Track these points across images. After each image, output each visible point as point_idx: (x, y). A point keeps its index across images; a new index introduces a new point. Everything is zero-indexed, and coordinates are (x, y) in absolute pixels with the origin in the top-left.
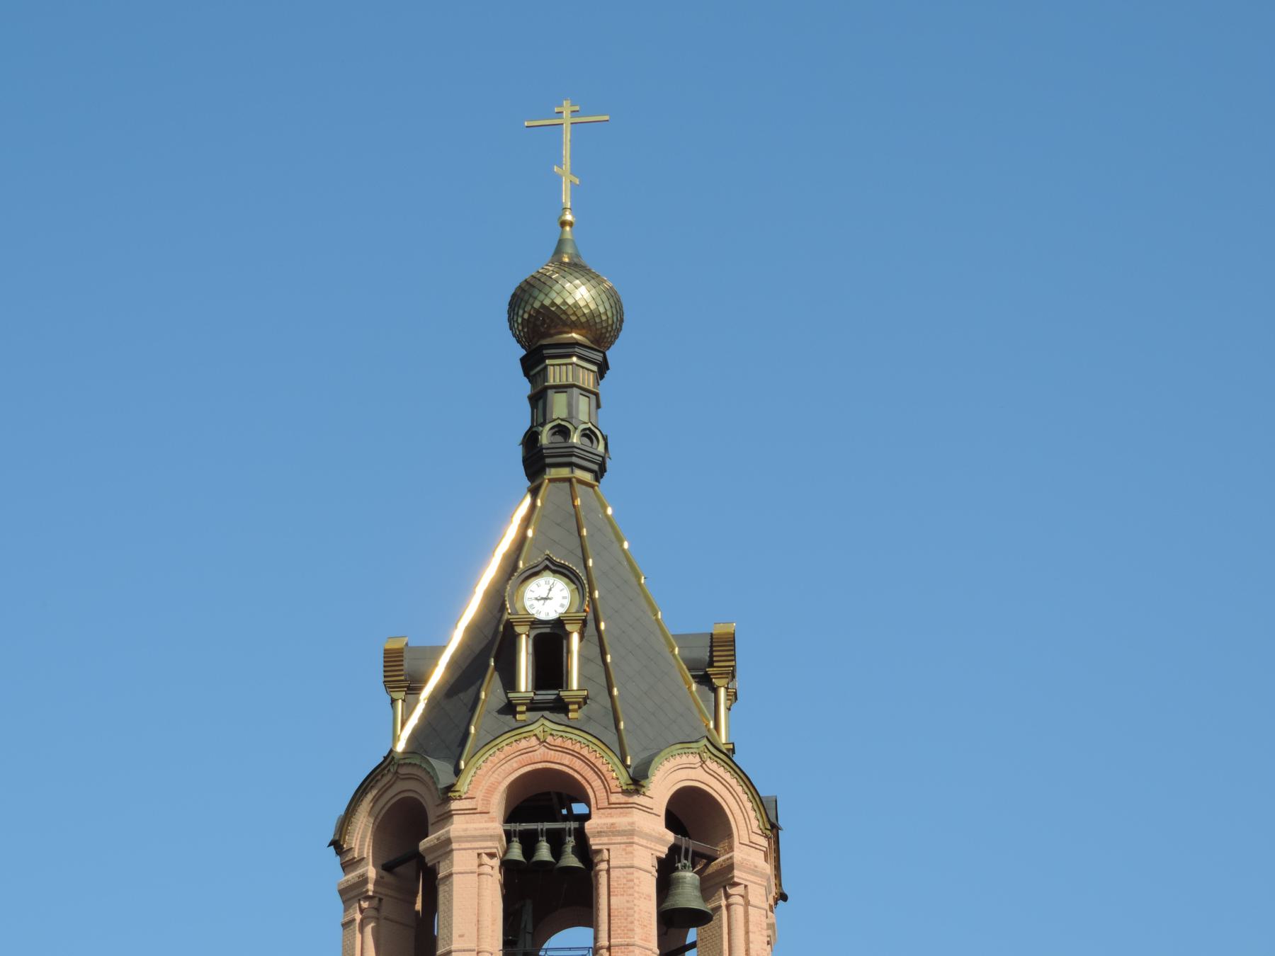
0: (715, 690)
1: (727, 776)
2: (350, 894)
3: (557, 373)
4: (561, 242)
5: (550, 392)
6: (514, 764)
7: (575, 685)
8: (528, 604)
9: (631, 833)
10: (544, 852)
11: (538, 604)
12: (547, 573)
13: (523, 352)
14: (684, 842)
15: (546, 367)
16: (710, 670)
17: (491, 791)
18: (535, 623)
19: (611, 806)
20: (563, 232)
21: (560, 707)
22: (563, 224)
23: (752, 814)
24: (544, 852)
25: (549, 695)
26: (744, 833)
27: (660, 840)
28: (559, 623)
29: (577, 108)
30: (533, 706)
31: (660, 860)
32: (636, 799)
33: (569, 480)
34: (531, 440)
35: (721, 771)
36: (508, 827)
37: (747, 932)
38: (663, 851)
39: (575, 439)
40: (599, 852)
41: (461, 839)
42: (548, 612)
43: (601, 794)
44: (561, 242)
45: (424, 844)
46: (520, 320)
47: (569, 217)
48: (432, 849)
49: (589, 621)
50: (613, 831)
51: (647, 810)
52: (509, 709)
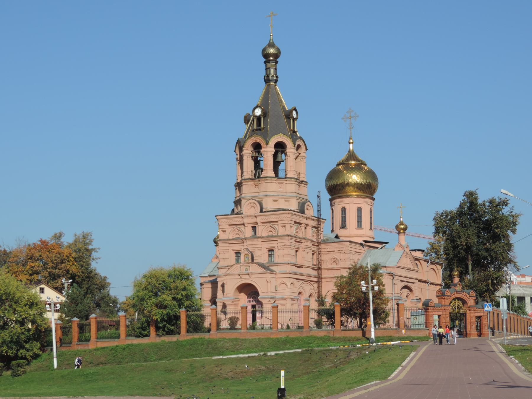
0: (291, 120)
2: (237, 159)
3: (268, 66)
4: (270, 40)
8: (255, 113)
9: (267, 151)
11: (257, 113)
14: (279, 149)
17: (248, 146)
18: (256, 116)
21: (260, 130)
22: (271, 36)
27: (273, 151)
28: (260, 116)
30: (257, 130)
32: (268, 146)
33: (269, 85)
38: (273, 153)
41: (244, 154)
44: (270, 40)
47: (271, 35)
49: (265, 114)
50: (264, 151)
51: (270, 147)
52: (253, 131)
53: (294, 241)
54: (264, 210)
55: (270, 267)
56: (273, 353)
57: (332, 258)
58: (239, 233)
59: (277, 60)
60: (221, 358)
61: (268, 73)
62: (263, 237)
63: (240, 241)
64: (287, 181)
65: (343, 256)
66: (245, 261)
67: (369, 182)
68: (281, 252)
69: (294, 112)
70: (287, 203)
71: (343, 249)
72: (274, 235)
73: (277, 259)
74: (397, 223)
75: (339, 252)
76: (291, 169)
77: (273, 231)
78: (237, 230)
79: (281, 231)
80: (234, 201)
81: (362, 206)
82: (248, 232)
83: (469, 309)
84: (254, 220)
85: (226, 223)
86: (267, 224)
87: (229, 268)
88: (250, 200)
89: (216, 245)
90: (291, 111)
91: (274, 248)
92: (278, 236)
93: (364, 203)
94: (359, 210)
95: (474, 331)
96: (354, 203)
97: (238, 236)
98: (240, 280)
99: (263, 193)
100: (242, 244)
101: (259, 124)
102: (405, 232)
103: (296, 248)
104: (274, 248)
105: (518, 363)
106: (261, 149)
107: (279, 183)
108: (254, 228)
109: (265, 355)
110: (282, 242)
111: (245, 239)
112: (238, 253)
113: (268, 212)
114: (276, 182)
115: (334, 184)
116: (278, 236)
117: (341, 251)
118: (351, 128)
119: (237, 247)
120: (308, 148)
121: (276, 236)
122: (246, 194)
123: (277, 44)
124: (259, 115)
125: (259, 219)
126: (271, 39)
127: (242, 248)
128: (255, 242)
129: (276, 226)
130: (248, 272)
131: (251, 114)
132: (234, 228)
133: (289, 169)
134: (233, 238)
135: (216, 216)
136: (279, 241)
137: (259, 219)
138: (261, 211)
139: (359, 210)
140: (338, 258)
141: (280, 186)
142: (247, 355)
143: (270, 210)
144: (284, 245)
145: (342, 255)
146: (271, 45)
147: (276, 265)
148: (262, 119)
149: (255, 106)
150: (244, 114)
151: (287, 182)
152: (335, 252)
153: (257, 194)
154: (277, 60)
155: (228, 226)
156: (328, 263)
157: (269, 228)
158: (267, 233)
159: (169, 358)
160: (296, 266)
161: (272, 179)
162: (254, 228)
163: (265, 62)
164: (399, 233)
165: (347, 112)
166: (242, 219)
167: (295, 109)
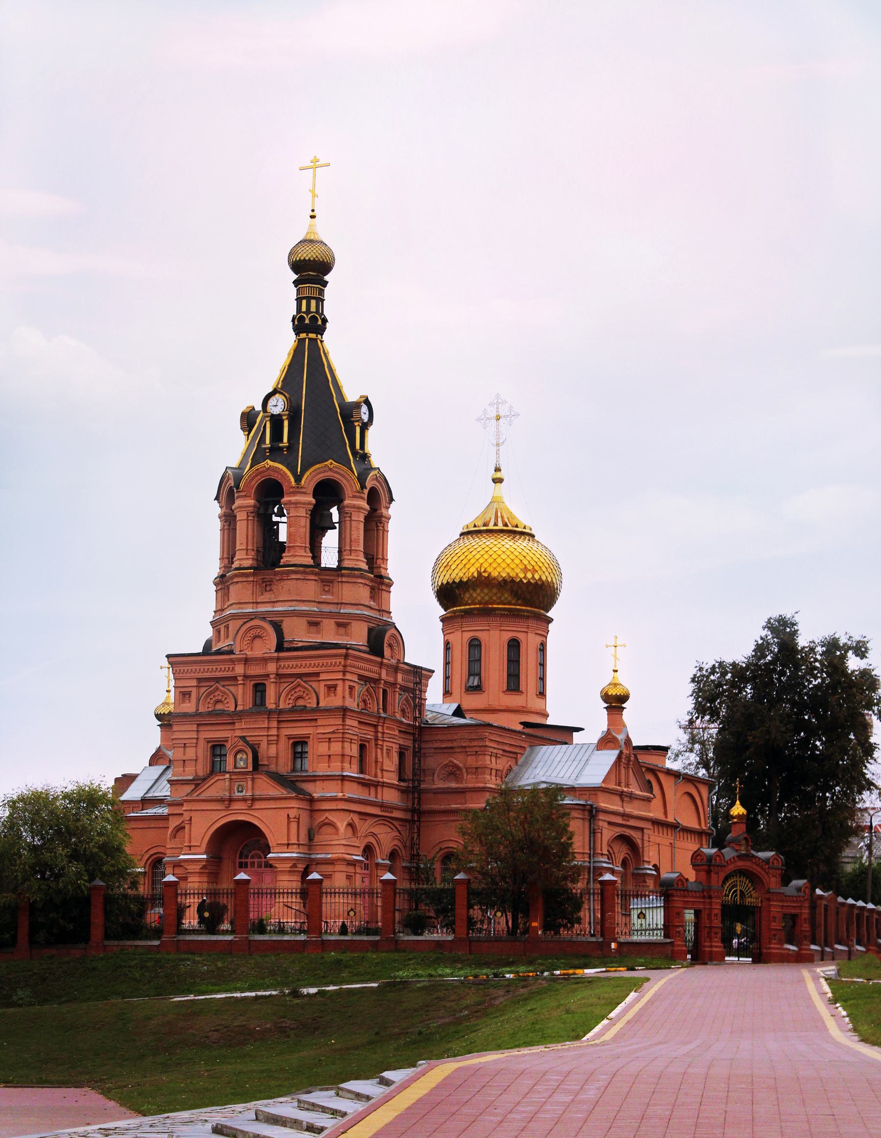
7: (285, 439)
13: (295, 277)
18: (272, 416)
25: (275, 444)
26: (350, 492)
27: (310, 503)
28: (280, 415)
37: (351, 531)
39: (307, 321)
42: (277, 411)
45: (233, 507)
50: (290, 503)
51: (305, 493)
53: (355, 724)
54: (286, 645)
55: (298, 784)
56: (313, 991)
57: (447, 765)
59: (326, 278)
60: (190, 1000)
61: (304, 309)
62: (281, 712)
64: (342, 575)
65: (471, 761)
66: (235, 768)
67: (540, 579)
69: (364, 409)
70: (342, 630)
71: (473, 744)
72: (308, 705)
73: (314, 765)
75: (463, 750)
80: (211, 619)
81: (521, 637)
82: (243, 697)
83: (767, 896)
86: (292, 680)
87: (198, 784)
88: (252, 619)
89: (160, 723)
90: (357, 405)
93: (526, 630)
94: (514, 645)
95: (719, 947)
96: (502, 628)
101: (277, 434)
103: (361, 740)
105: (844, 1017)
106: (283, 497)
107: (322, 581)
108: (259, 690)
109: (295, 994)
110: (328, 725)
111: (238, 715)
112: (217, 748)
114: (313, 577)
115: (454, 582)
117: (467, 750)
118: (498, 445)
120: (394, 497)
121: (314, 710)
124: (278, 413)
131: (258, 408)
136: (319, 723)
137: (272, 668)
138: (280, 648)
139: (514, 645)
141: (327, 588)
142: (253, 994)
143: (300, 644)
144: (333, 732)
145: (469, 758)
147: (314, 779)
148: (286, 423)
149: (271, 390)
150: (243, 408)
151: (344, 579)
154: (326, 278)
155: (194, 683)
156: (436, 775)
157: (297, 690)
159: (64, 999)
160: (359, 783)
161: (308, 570)
162: (259, 690)
163: (296, 283)
165: (491, 404)
167: (367, 402)
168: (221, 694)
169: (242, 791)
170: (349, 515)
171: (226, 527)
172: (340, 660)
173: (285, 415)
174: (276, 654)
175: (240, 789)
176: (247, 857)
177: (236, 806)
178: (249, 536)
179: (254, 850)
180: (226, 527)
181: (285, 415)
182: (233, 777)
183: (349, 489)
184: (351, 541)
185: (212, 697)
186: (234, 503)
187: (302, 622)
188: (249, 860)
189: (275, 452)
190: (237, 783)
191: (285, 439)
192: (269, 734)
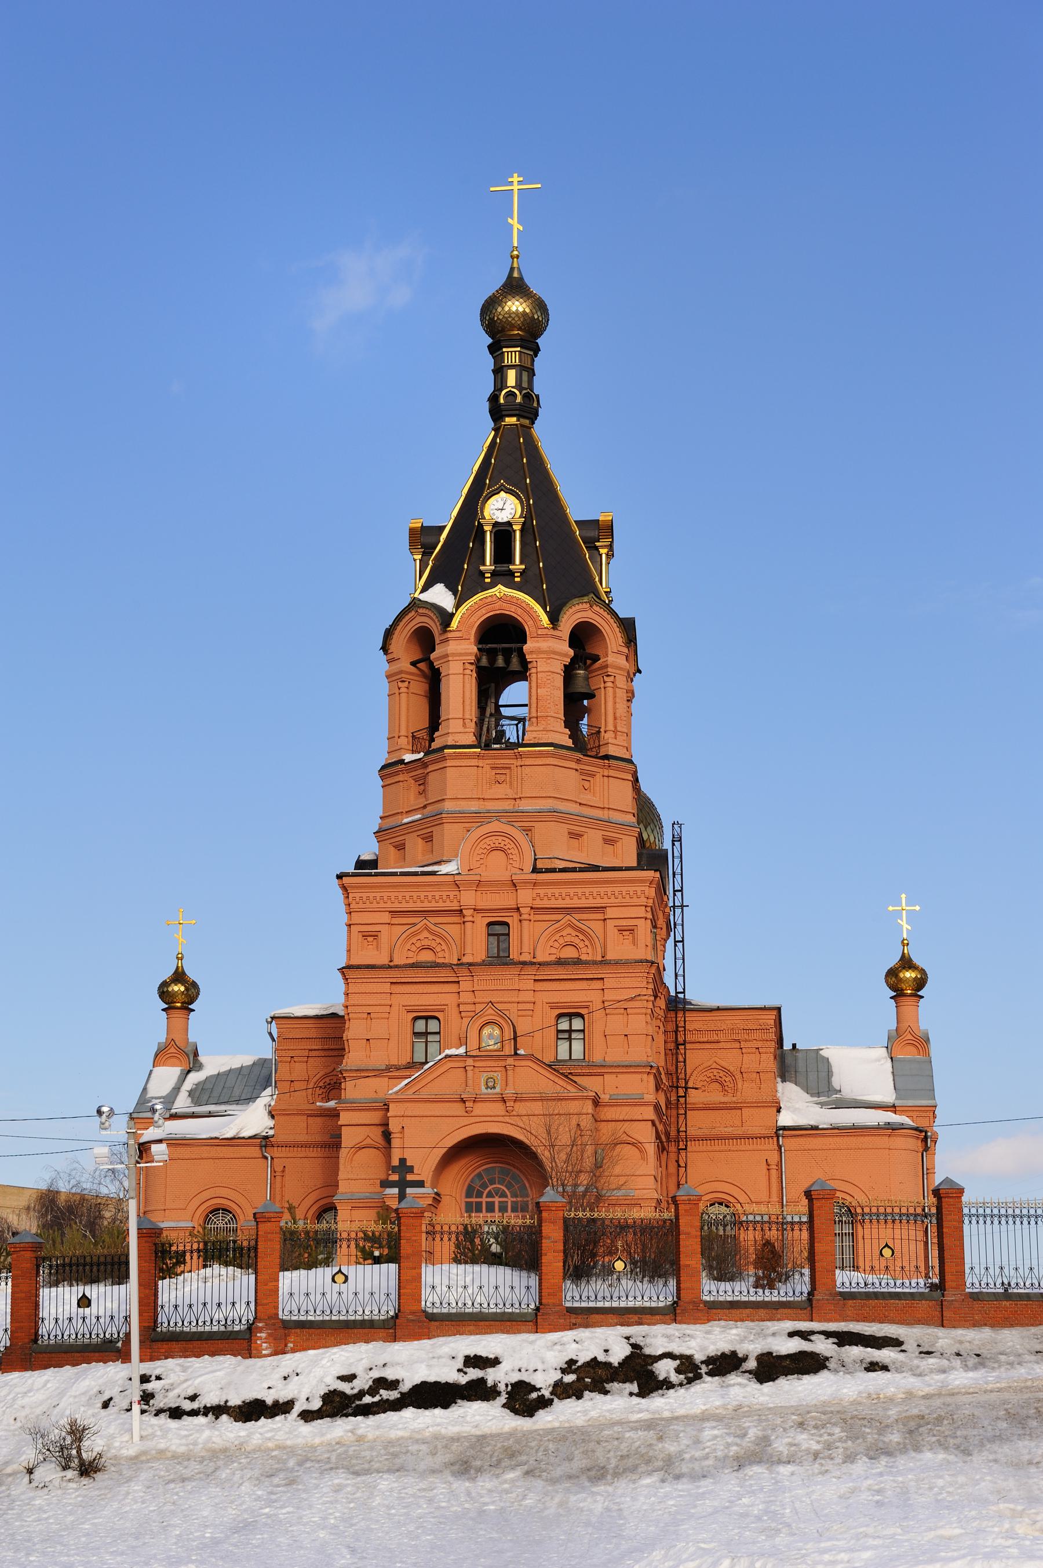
1: (605, 614)
4: (512, 269)
5: (505, 369)
6: (483, 611)
10: (500, 662)
11: (498, 513)
12: (502, 492)
13: (490, 341)
15: (503, 353)
16: (597, 544)
19: (538, 636)
20: (513, 262)
22: (512, 257)
23: (619, 635)
24: (500, 662)
25: (502, 568)
27: (566, 655)
29: (521, 179)
31: (565, 665)
34: (493, 399)
35: (601, 611)
36: (480, 646)
39: (519, 400)
40: (530, 662)
41: (454, 655)
42: (503, 517)
43: (533, 629)
45: (433, 656)
46: (487, 318)
48: (438, 659)
50: (539, 651)
58: (433, 944)
63: (444, 975)
68: (616, 1023)
74: (893, 960)
75: (737, 1045)
76: (619, 729)
77: (581, 945)
78: (426, 934)
79: (619, 949)
84: (505, 899)
85: (382, 905)
86: (560, 917)
91: (587, 1007)
92: (604, 962)
97: (426, 957)
98: (467, 1121)
99: (530, 801)
100: (453, 988)
102: (919, 993)
104: (587, 1007)
113: (553, 870)
114: (573, 765)
116: (604, 962)
119: (427, 998)
122: (463, 803)
123: (535, 287)
124: (505, 520)
125: (525, 897)
126: (515, 265)
127: (451, 1000)
128: (507, 979)
129: (597, 927)
130: (498, 1090)
132: (415, 924)
133: (611, 727)
134: (410, 961)
135: (340, 877)
136: (608, 983)
140: (732, 1069)
141: (586, 785)
144: (632, 999)
146: (515, 286)
151: (612, 773)
152: (721, 1045)
153: (507, 805)
155: (386, 917)
157: (564, 933)
158: (553, 951)
164: (899, 994)
166: (452, 894)
168: (431, 937)
169: (494, 1088)
170: (611, 679)
171: (403, 690)
172: (643, 888)
173: (517, 523)
174: (534, 876)
175: (490, 1084)
176: (480, 1195)
177: (479, 1109)
178: (468, 702)
179: (492, 1182)
180: (403, 690)
181: (517, 523)
182: (477, 1064)
183: (613, 641)
184: (615, 718)
185: (414, 940)
186: (434, 650)
187: (563, 829)
188: (484, 1200)
189: (503, 576)
190: (485, 1074)
191: (517, 561)
192: (520, 1000)
